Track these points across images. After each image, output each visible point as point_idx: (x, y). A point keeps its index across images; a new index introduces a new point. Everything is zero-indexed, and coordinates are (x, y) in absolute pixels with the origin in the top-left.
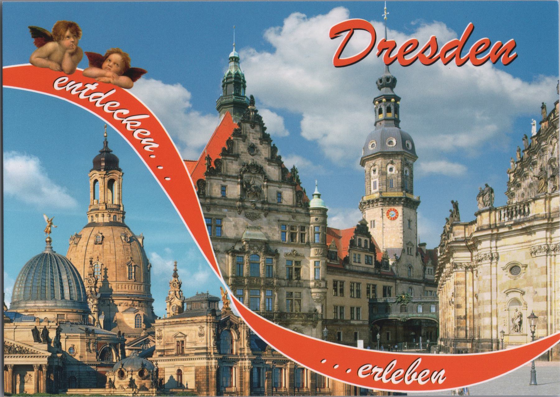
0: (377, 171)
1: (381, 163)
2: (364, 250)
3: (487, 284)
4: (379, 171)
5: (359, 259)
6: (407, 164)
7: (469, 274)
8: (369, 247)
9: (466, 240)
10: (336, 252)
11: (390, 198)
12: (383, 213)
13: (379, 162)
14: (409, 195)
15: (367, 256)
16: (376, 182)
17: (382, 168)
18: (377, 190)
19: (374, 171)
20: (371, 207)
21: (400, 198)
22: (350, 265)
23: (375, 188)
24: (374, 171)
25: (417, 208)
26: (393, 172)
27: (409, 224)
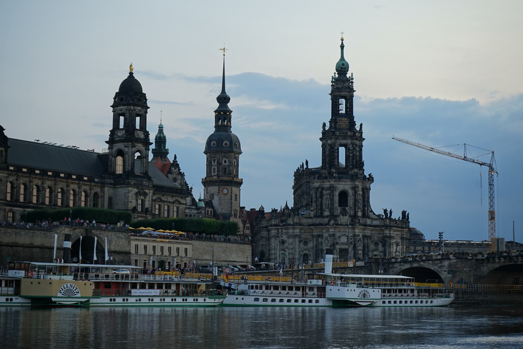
0: (216, 161)
3: (273, 247)
6: (235, 158)
7: (267, 242)
9: (266, 227)
11: (224, 181)
12: (219, 190)
14: (235, 179)
18: (216, 174)
19: (214, 161)
23: (214, 172)
24: (214, 161)
26: (227, 164)
27: (236, 198)
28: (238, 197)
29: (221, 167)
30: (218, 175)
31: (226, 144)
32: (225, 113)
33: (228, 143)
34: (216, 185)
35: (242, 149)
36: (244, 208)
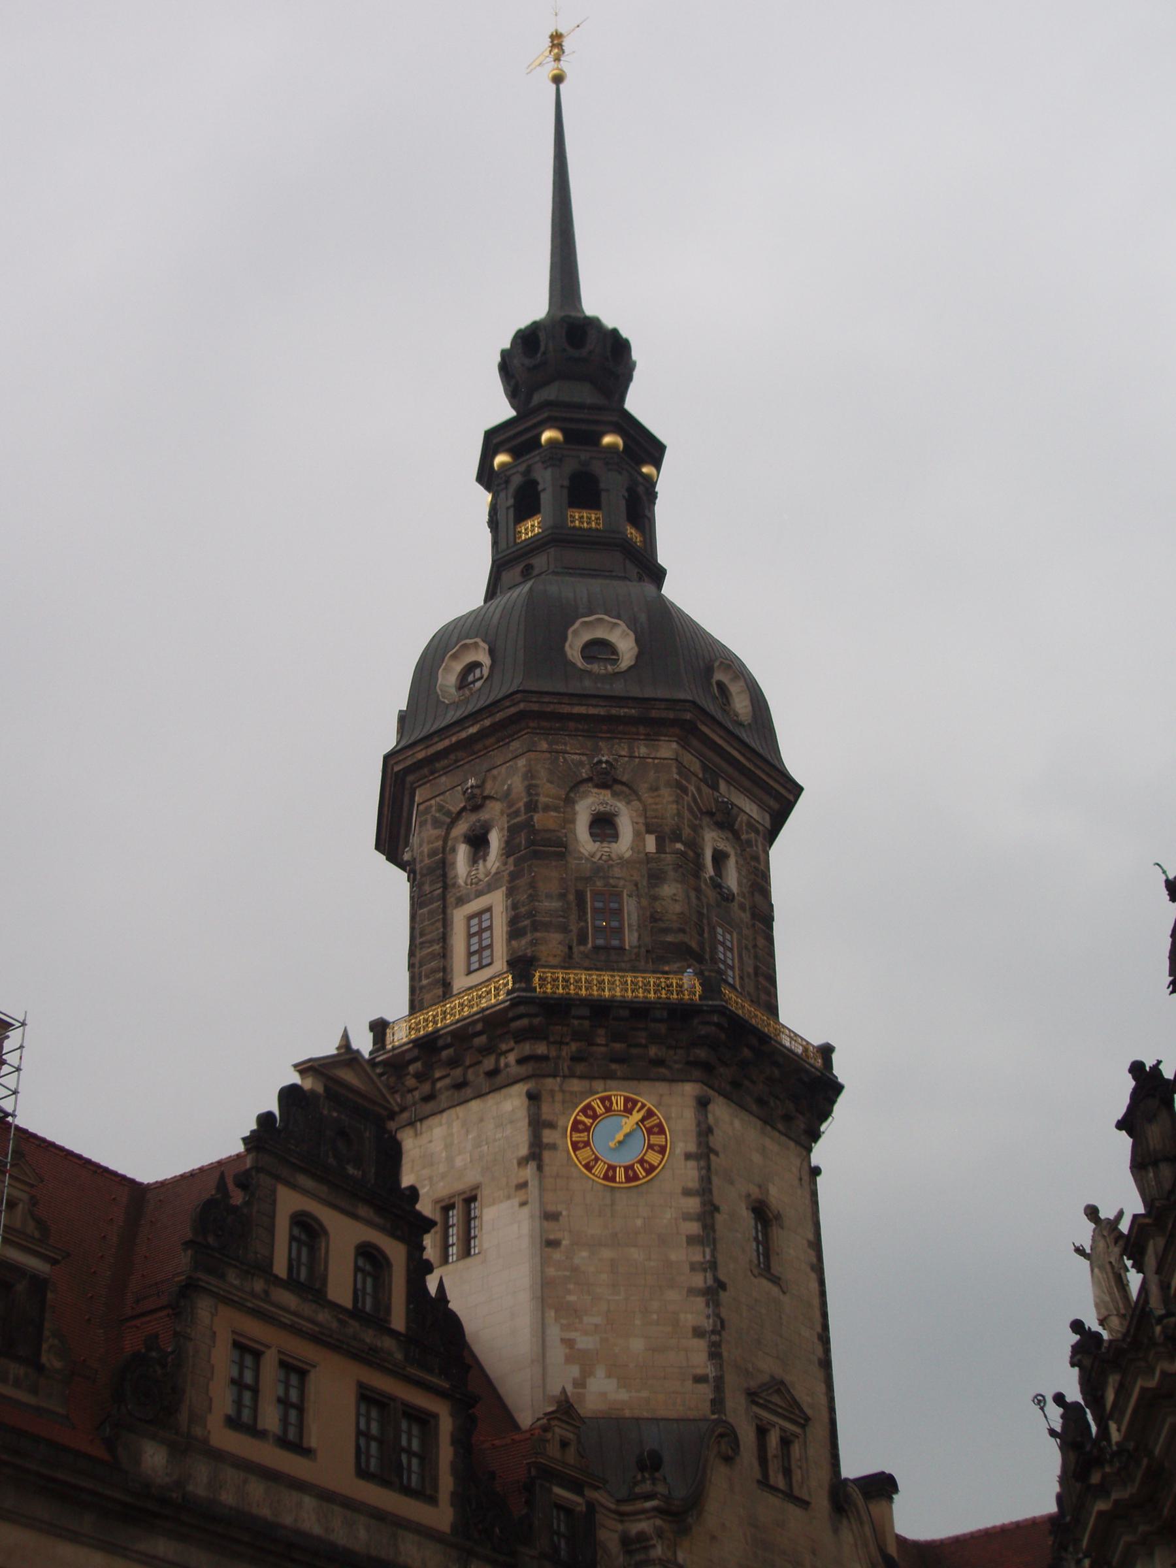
0: (495, 839)
1: (530, 775)
2: (352, 1334)
4: (513, 832)
5: (294, 1408)
6: (725, 819)
8: (398, 1322)
10: (39, 1284)
11: (600, 1010)
12: (537, 1125)
13: (512, 774)
15: (367, 1397)
16: (489, 909)
17: (532, 807)
19: (478, 842)
20: (443, 1098)
21: (680, 1014)
22: (186, 1446)
24: (478, 842)
25: (815, 1136)
26: (624, 844)
28: (790, 1246)
29: (550, 878)
30: (521, 966)
31: (599, 649)
32: (581, 436)
33: (625, 645)
34: (496, 1081)
35: (795, 757)
36: (882, 1486)
